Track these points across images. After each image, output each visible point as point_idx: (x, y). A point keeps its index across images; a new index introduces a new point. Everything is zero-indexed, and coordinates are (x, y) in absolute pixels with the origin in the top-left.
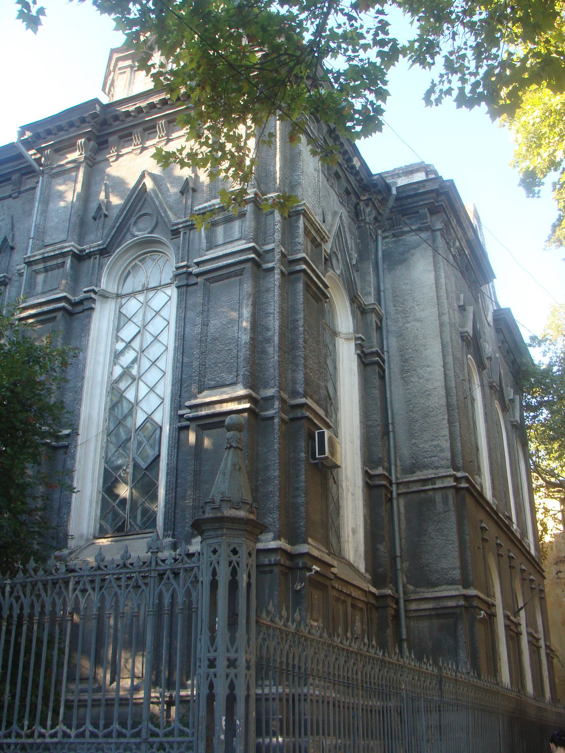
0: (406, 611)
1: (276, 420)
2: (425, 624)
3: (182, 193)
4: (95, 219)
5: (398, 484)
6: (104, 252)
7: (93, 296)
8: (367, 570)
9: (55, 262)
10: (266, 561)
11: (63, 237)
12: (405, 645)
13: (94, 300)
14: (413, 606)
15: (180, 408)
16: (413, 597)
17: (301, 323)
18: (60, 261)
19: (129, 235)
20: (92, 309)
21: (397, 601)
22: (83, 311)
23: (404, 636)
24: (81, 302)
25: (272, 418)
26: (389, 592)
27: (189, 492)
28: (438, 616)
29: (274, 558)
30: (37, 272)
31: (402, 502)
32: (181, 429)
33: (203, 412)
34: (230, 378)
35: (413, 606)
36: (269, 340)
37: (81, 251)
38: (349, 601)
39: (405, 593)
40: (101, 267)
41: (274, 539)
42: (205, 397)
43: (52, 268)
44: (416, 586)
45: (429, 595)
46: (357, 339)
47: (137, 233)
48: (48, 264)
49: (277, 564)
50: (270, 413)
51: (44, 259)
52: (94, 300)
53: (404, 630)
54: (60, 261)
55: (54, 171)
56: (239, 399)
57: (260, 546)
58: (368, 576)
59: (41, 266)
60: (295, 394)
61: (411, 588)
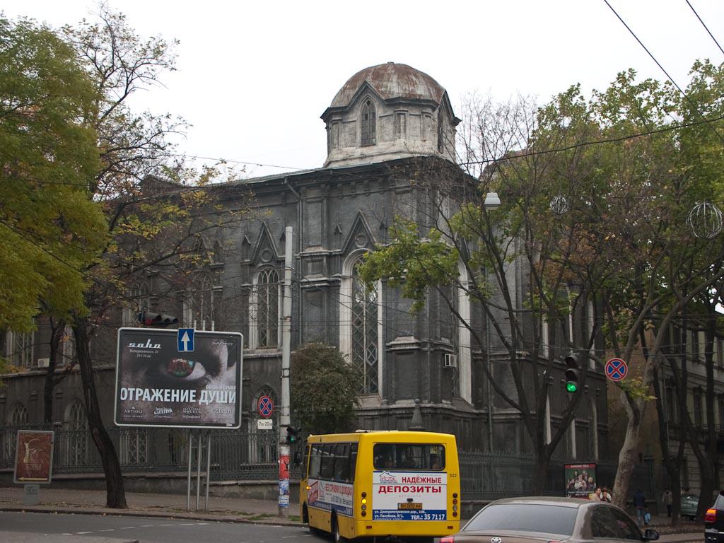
0: (492, 419)
1: (428, 353)
2: (501, 426)
3: (380, 228)
4: (335, 234)
5: (490, 356)
6: (343, 255)
7: (340, 279)
8: (472, 402)
9: (317, 258)
10: (425, 411)
11: (319, 243)
12: (491, 435)
13: (340, 281)
14: (495, 418)
15: (387, 342)
16: (496, 412)
17: (439, 304)
18: (320, 258)
19: (354, 247)
20: (340, 286)
21: (487, 415)
22: (335, 286)
23: (491, 432)
24: (333, 281)
25: (427, 352)
26: (483, 411)
27: (393, 382)
28: (508, 423)
29: (429, 410)
30: (308, 262)
31: (492, 365)
32: (387, 352)
33: (398, 348)
34: (409, 332)
35: (495, 418)
36: (425, 315)
37: (330, 253)
38: (462, 420)
39: (492, 410)
40: (342, 262)
41: (429, 402)
42: (398, 341)
43: (316, 261)
44: (498, 407)
45: (502, 412)
46: (470, 283)
47: (358, 246)
48: (314, 259)
49: (430, 413)
50: (426, 349)
51: (311, 256)
52: (340, 281)
53: (491, 428)
54: (320, 258)
55: (308, 200)
56: (413, 344)
57: (422, 405)
58: (473, 405)
59: (310, 259)
60: (436, 338)
61: (495, 408)
